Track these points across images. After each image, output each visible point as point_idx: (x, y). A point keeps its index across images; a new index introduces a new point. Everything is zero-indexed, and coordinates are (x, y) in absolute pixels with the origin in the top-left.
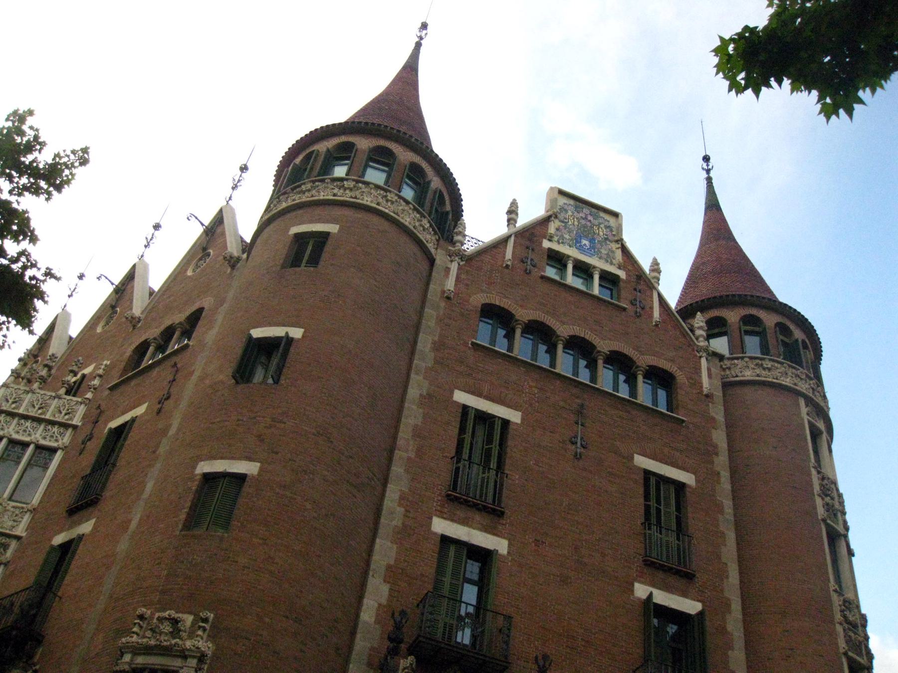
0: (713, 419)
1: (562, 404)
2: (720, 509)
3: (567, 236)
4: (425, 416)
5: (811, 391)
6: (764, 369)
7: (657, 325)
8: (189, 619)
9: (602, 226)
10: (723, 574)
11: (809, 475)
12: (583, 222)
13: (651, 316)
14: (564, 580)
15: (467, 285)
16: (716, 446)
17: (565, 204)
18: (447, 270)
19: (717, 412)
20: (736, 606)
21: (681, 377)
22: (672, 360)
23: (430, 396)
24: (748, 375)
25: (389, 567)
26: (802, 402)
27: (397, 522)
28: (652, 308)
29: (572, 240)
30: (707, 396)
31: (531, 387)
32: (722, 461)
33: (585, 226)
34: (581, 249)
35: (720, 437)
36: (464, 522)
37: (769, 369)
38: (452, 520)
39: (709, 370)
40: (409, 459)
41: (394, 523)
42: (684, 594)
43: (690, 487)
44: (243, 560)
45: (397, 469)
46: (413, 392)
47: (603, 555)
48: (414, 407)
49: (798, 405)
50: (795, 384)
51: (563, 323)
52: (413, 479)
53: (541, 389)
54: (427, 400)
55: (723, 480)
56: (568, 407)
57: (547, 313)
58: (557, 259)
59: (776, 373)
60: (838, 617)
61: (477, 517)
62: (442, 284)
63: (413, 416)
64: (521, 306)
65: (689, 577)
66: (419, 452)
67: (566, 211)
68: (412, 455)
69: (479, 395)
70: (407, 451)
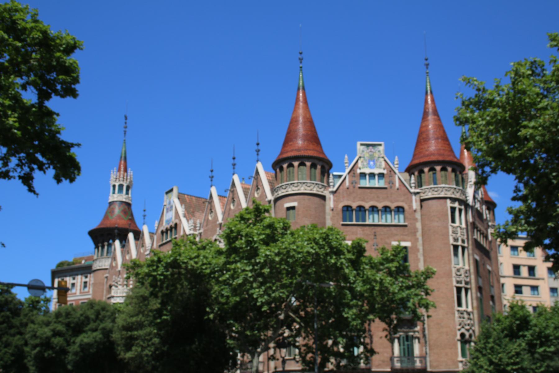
11: (448, 229)
12: (370, 153)
13: (395, 186)
18: (330, 198)
19: (418, 216)
21: (406, 207)
22: (403, 201)
24: (430, 195)
32: (419, 234)
33: (371, 155)
35: (419, 225)
51: (367, 202)
58: (363, 175)
60: (454, 275)
62: (329, 204)
64: (354, 202)
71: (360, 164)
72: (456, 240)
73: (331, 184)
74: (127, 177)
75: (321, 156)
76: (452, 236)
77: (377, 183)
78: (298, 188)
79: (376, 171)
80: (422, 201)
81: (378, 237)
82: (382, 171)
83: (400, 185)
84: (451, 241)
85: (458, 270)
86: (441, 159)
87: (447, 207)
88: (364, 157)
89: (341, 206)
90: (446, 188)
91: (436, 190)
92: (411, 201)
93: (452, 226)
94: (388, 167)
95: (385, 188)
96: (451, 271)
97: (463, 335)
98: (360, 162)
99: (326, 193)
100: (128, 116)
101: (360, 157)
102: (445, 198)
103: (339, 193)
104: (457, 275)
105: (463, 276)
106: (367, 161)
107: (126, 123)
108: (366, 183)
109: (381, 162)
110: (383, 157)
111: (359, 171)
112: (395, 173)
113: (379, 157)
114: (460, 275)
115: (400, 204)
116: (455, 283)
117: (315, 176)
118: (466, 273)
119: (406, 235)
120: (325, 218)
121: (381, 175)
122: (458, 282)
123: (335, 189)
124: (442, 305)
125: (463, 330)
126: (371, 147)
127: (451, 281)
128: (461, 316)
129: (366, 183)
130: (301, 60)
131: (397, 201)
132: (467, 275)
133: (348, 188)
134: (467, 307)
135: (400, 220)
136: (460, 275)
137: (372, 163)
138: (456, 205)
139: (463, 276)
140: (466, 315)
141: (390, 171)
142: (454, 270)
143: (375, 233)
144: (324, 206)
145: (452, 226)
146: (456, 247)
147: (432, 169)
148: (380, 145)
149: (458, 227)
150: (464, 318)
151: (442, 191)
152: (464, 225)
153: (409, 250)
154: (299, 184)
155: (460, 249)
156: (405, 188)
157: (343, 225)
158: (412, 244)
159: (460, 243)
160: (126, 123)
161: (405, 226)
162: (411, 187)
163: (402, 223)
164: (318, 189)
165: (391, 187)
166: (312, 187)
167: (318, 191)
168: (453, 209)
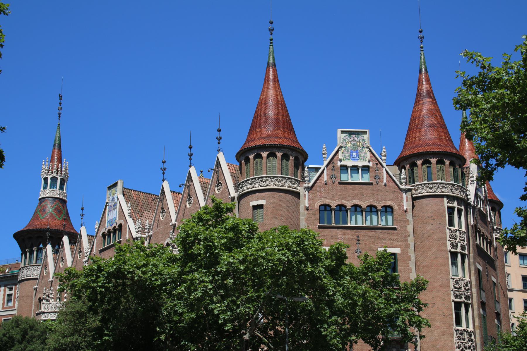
0: (408, 220)
1: (351, 237)
2: (409, 258)
3: (347, 155)
6: (430, 188)
7: (385, 185)
12: (353, 142)
13: (383, 181)
15: (313, 199)
16: (409, 233)
17: (344, 136)
19: (409, 217)
21: (395, 207)
22: (391, 200)
24: (423, 193)
26: (445, 199)
28: (383, 177)
29: (349, 156)
30: (406, 211)
31: (340, 235)
34: (353, 159)
35: (410, 228)
37: (432, 188)
39: (407, 197)
43: (398, 254)
49: (444, 201)
53: (344, 234)
56: (353, 238)
57: (343, 199)
58: (344, 168)
59: (434, 189)
62: (304, 203)
64: (333, 200)
67: (345, 140)
71: (340, 155)
72: (454, 246)
73: (306, 179)
74: (61, 169)
75: (294, 145)
76: (450, 241)
77: (359, 178)
78: (267, 183)
79: (360, 164)
80: (414, 199)
81: (361, 241)
82: (366, 163)
83: (388, 181)
84: (449, 248)
85: (457, 282)
86: (436, 149)
87: (445, 207)
88: (345, 147)
89: (317, 205)
90: (442, 185)
91: (431, 186)
92: (402, 199)
93: (450, 229)
94: (374, 158)
95: (371, 184)
96: (449, 283)
98: (340, 152)
99: (301, 189)
100: (62, 95)
101: (341, 147)
102: (442, 196)
103: (316, 189)
104: (456, 288)
105: (463, 289)
106: (349, 153)
107: (60, 104)
108: (346, 177)
109: (365, 153)
110: (368, 147)
111: (339, 164)
113: (363, 147)
114: (460, 288)
115: (388, 203)
116: (453, 298)
117: (287, 169)
118: (467, 285)
119: (395, 240)
120: (298, 219)
121: (366, 169)
122: (456, 296)
123: (310, 185)
124: (438, 324)
126: (354, 136)
127: (449, 295)
128: (461, 336)
129: (346, 177)
130: (271, 30)
131: (385, 199)
132: (467, 288)
133: (326, 184)
134: (468, 326)
135: (389, 221)
136: (460, 288)
137: (354, 154)
138: (455, 204)
139: (463, 289)
140: (466, 337)
141: (377, 164)
142: (452, 282)
143: (358, 237)
144: (298, 204)
145: (450, 229)
146: (454, 255)
147: (427, 162)
148: (365, 133)
149: (457, 230)
150: (464, 339)
151: (438, 188)
152: (464, 229)
153: (399, 258)
154: (268, 178)
155: (459, 256)
157: (320, 227)
158: (401, 250)
159: (459, 250)
160: (60, 104)
161: (395, 229)
162: (401, 183)
163: (390, 225)
164: (291, 185)
166: (283, 182)
167: (290, 187)
168: (451, 210)
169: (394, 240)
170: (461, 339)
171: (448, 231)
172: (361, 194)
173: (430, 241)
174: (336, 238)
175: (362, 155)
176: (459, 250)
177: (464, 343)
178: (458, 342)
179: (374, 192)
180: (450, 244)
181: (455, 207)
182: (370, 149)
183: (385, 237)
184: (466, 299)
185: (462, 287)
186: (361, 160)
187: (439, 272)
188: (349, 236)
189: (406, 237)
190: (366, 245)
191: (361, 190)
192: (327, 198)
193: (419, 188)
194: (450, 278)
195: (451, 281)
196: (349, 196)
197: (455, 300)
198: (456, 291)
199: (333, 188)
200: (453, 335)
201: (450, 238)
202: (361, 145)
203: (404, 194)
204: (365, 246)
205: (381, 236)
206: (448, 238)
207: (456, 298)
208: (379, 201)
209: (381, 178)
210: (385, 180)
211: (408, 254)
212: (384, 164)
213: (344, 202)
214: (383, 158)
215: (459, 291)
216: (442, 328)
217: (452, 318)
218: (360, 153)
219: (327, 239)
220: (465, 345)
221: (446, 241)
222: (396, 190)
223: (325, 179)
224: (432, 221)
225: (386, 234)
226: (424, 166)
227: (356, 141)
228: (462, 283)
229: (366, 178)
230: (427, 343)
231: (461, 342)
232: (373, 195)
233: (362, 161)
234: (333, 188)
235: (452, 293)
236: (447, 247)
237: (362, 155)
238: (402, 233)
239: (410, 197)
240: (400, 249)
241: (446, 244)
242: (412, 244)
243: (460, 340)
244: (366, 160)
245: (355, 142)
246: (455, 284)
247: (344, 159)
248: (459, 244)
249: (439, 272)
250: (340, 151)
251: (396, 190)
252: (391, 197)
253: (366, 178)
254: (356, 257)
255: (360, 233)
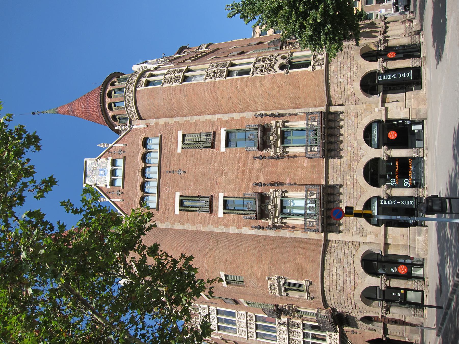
0: (155, 123)
2: (187, 122)
3: (102, 179)
4: (187, 223)
5: (132, 85)
6: (130, 103)
7: (126, 145)
8: (269, 282)
9: (92, 166)
10: (209, 121)
11: (165, 88)
12: (93, 174)
13: (123, 147)
14: (226, 174)
16: (165, 123)
19: (152, 122)
20: (220, 116)
21: (144, 136)
23: (180, 222)
24: (134, 109)
25: (237, 228)
26: (138, 89)
27: (224, 227)
28: (120, 147)
29: (103, 178)
30: (148, 126)
31: (165, 189)
32: (171, 121)
34: (106, 174)
35: (162, 121)
36: (217, 207)
38: (218, 210)
39: (137, 125)
40: (203, 226)
41: (224, 228)
42: (220, 135)
43: (183, 133)
44: (250, 272)
45: (207, 229)
46: (181, 227)
47: (214, 162)
48: (185, 226)
49: (139, 90)
50: (132, 92)
52: (209, 224)
53: (165, 186)
54: (181, 222)
55: (177, 120)
56: (168, 176)
57: (136, 185)
58: (113, 183)
59: (130, 100)
60: (213, 80)
61: (214, 203)
63: (188, 227)
64: (137, 194)
65: (214, 133)
66: (200, 223)
67: (91, 180)
68: (201, 225)
69: (174, 206)
70: (200, 227)
71: (101, 185)
76: (173, 83)
80: (140, 118)
82: (109, 162)
83: (123, 142)
84: (178, 84)
87: (145, 89)
91: (127, 103)
92: (138, 129)
93: (163, 84)
94: (106, 155)
95: (125, 157)
97: (282, 67)
104: (214, 76)
106: (101, 177)
110: (97, 161)
111: (108, 187)
112: (112, 147)
113: (97, 164)
114: (214, 72)
115: (141, 142)
116: (222, 79)
118: (213, 66)
121: (114, 163)
122: (221, 76)
124: (247, 93)
125: (276, 67)
126: (88, 172)
127: (220, 82)
131: (138, 145)
133: (123, 200)
136: (214, 72)
138: (143, 80)
139: (215, 70)
141: (109, 152)
145: (163, 84)
146: (185, 79)
148: (86, 162)
150: (262, 67)
151: (129, 95)
155: (187, 74)
156: (126, 136)
158: (180, 130)
161: (161, 136)
165: (125, 152)
169: (171, 137)
170: (262, 69)
171: (164, 86)
172: (133, 167)
173: (173, 102)
174: (168, 193)
175: (103, 165)
176: (181, 75)
177: (265, 66)
178: (265, 71)
179: (132, 155)
180: (176, 83)
181: (146, 80)
182: (98, 158)
183: (169, 145)
184: (224, 66)
185: (214, 70)
186: (106, 167)
187: (199, 93)
188: (167, 181)
189: (169, 125)
190: (174, 165)
191: (130, 167)
192: (135, 200)
193: (131, 113)
194: (204, 82)
195: (207, 81)
196: (134, 179)
197: (225, 76)
198: (216, 76)
199: (127, 194)
200: (257, 77)
201: (170, 83)
202: (96, 167)
203: (134, 127)
204: (175, 165)
205: (167, 149)
206: (169, 85)
207: (223, 76)
208: (139, 151)
209: (121, 148)
210: (122, 145)
211: (184, 123)
212: (110, 145)
213: (139, 184)
214: (106, 146)
215: (217, 73)
216: (251, 88)
217: (242, 78)
218: (101, 168)
219: (169, 202)
220: (267, 65)
221: (173, 86)
222: (131, 134)
223: (119, 200)
224: (156, 100)
225: (166, 144)
226: (114, 110)
227: (92, 171)
228: (210, 70)
229: (120, 162)
230: (266, 104)
231: (265, 68)
232: (133, 156)
233: (107, 166)
234: (127, 194)
235: (218, 79)
236: (177, 86)
237: (103, 165)
238: (166, 129)
239: (136, 122)
240: (179, 131)
241: (175, 86)
242: (175, 119)
243: (262, 70)
244: (107, 162)
245: (94, 171)
246: (210, 77)
247: (106, 183)
248: (176, 75)
249: (199, 93)
250: (99, 186)
251: (131, 134)
252: (136, 139)
253: (120, 162)
254: (185, 175)
255: (165, 170)
